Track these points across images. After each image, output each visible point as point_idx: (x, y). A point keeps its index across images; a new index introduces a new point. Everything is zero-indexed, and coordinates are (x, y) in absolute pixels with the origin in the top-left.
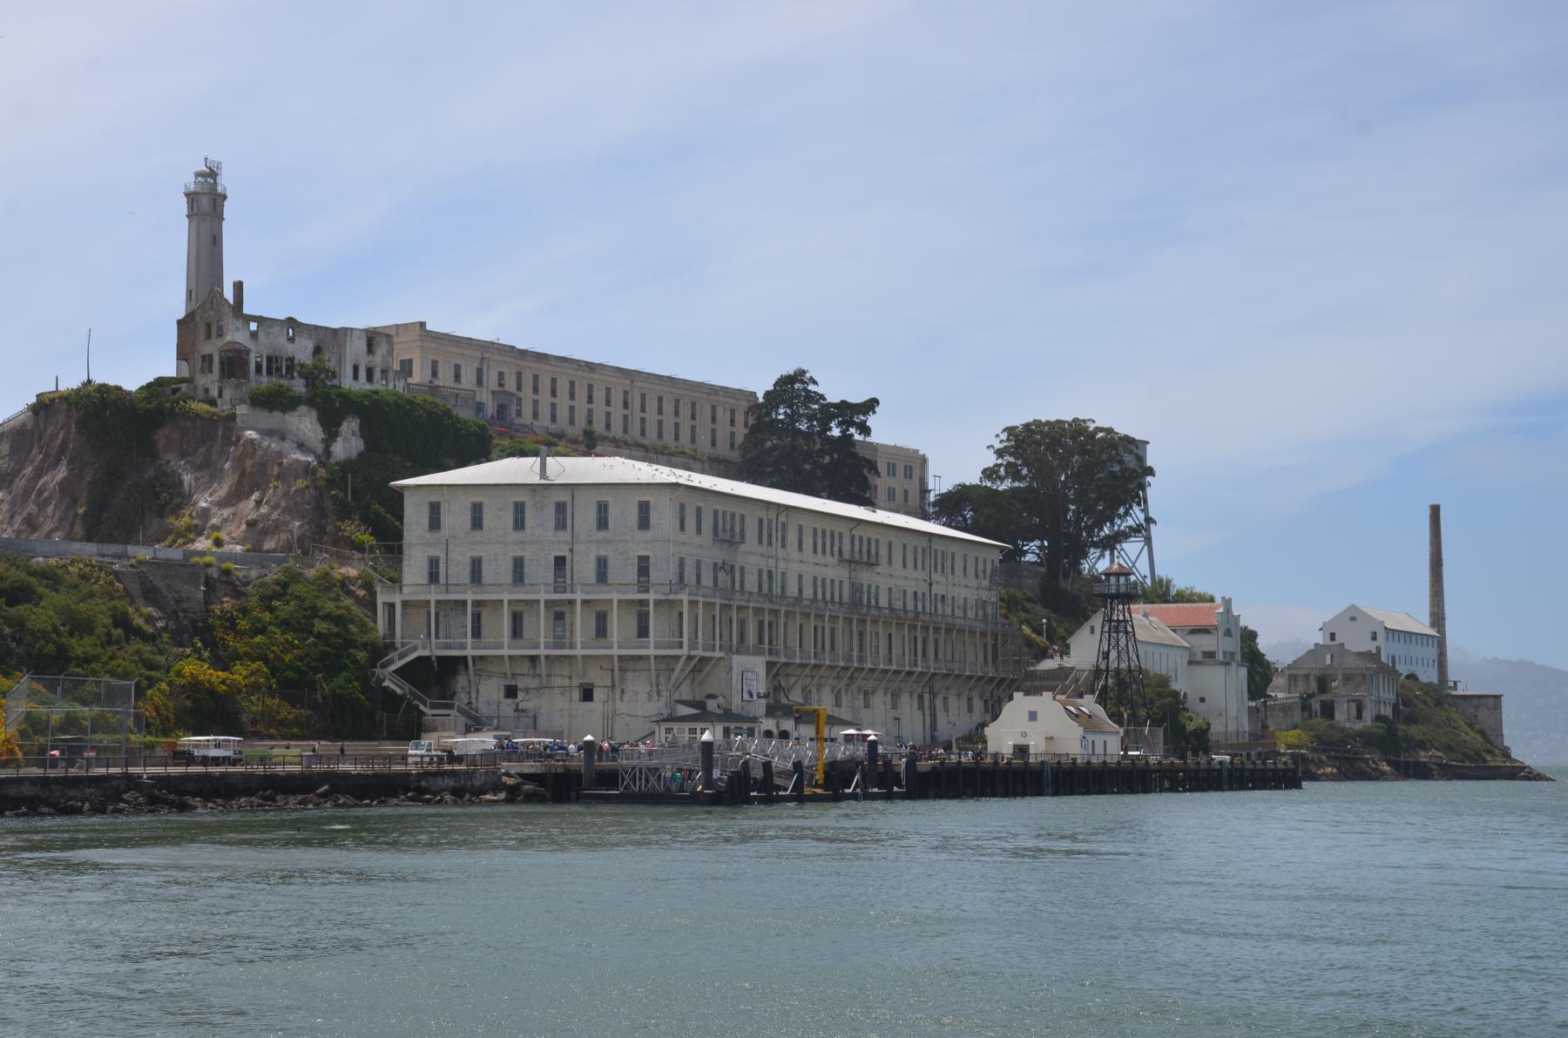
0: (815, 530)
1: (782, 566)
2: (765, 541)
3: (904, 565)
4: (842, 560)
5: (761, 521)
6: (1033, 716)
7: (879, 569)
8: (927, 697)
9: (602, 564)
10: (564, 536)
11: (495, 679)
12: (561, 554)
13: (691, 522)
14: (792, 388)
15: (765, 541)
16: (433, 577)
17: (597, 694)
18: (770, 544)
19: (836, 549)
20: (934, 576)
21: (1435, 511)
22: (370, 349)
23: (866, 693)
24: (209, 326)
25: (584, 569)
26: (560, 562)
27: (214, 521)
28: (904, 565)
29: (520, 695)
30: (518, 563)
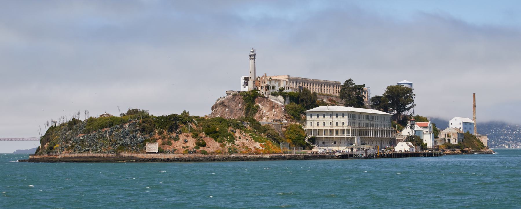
1: (361, 122)
3: (377, 120)
6: (402, 145)
8: (381, 142)
9: (337, 123)
11: (321, 141)
14: (349, 82)
16: (311, 125)
17: (337, 143)
20: (382, 121)
21: (474, 94)
22: (287, 85)
25: (334, 124)
26: (331, 123)
28: (377, 120)
29: (325, 143)
30: (324, 123)
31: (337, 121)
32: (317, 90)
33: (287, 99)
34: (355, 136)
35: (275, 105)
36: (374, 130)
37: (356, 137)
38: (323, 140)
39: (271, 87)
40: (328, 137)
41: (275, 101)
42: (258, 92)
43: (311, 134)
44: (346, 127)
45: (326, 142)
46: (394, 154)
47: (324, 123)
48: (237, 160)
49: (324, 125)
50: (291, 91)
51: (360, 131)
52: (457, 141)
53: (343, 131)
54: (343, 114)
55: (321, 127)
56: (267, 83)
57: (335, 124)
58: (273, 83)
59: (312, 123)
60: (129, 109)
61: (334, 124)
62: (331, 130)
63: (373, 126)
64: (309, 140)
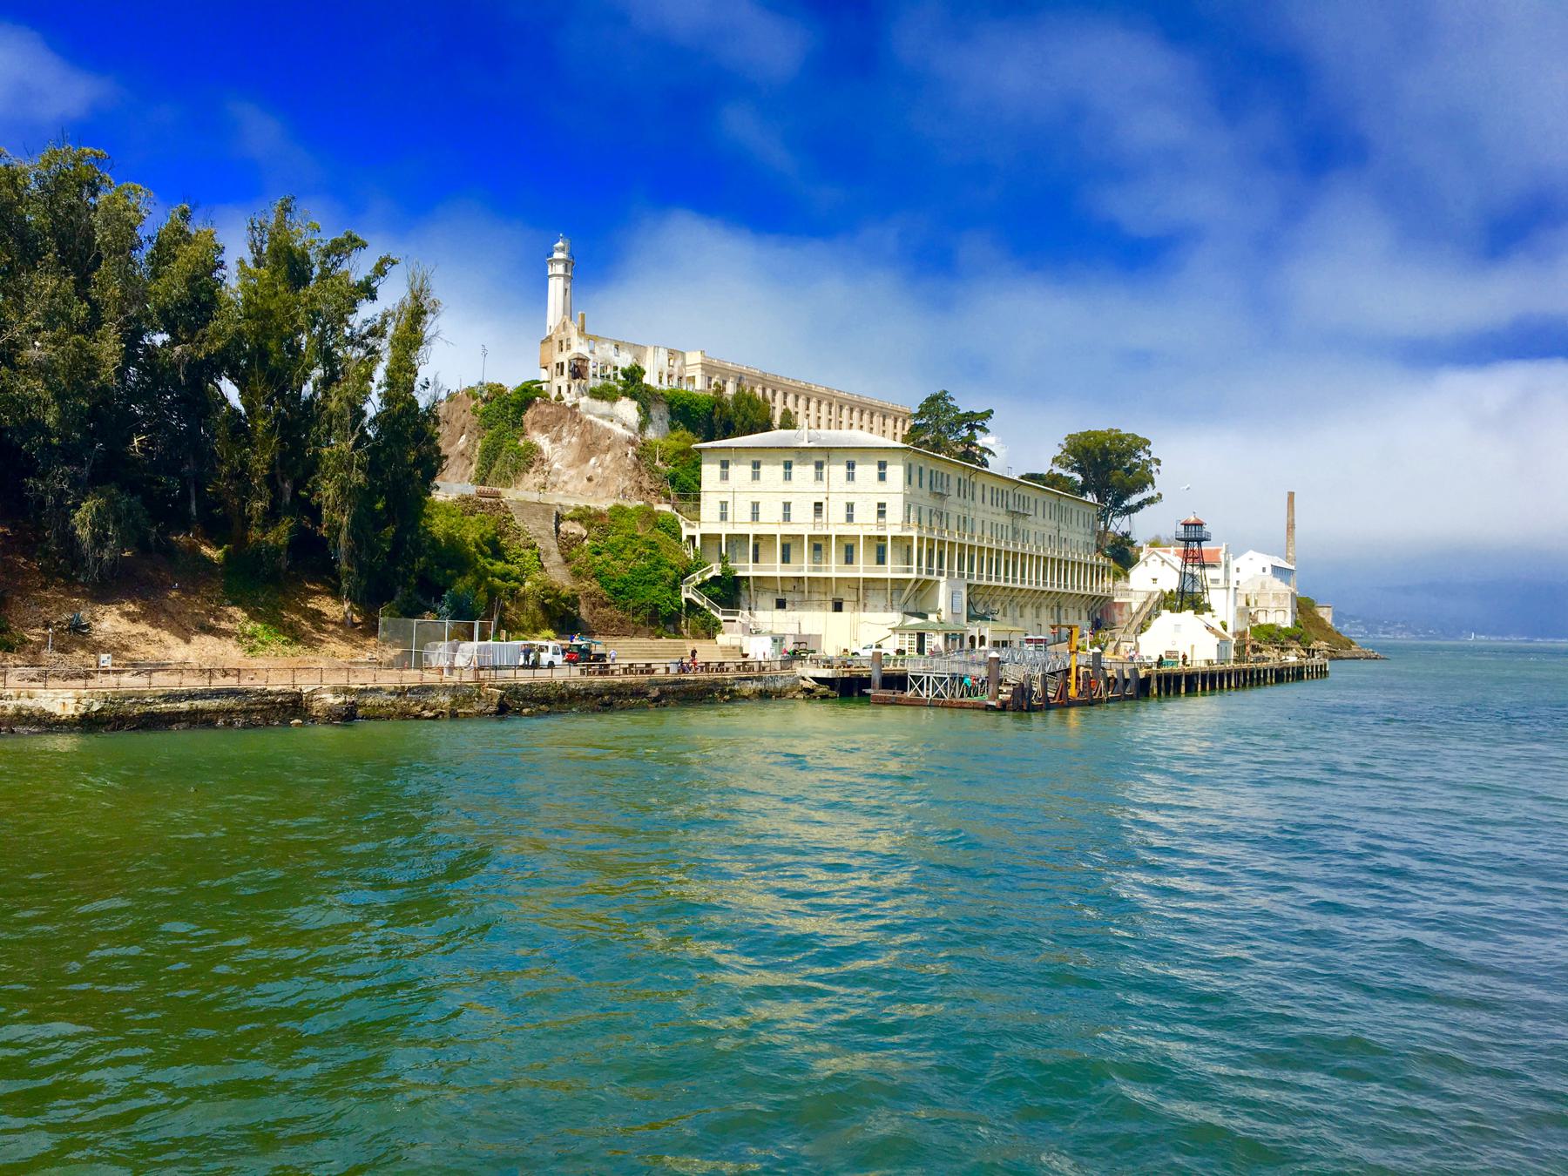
0: (992, 488)
1: (972, 513)
2: (962, 495)
4: (1008, 511)
5: (960, 480)
7: (1030, 518)
8: (1056, 609)
9: (850, 507)
10: (822, 486)
11: (769, 594)
13: (915, 478)
15: (962, 495)
16: (723, 517)
18: (965, 497)
19: (1005, 502)
21: (1291, 495)
24: (561, 342)
25: (836, 512)
26: (818, 506)
27: (565, 478)
30: (787, 506)
34: (940, 573)
35: (598, 438)
36: (1031, 556)
37: (943, 579)
41: (600, 422)
42: (541, 388)
44: (894, 526)
46: (1159, 678)
47: (787, 506)
49: (787, 517)
51: (967, 554)
53: (879, 547)
55: (771, 524)
57: (842, 513)
59: (726, 502)
61: (836, 512)
63: (1026, 539)
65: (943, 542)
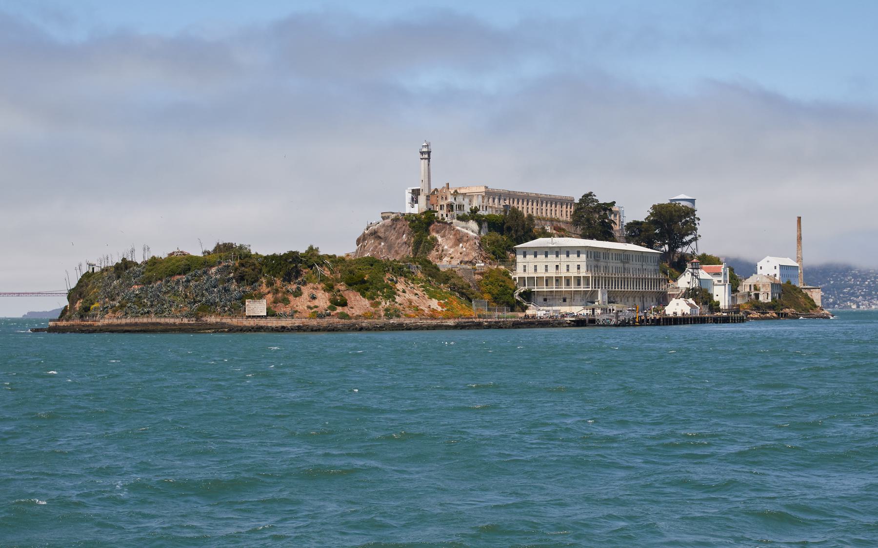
1: (608, 264)
6: (678, 304)
9: (568, 266)
12: (557, 264)
16: (525, 270)
17: (567, 300)
21: (799, 218)
23: (628, 298)
25: (563, 268)
26: (557, 266)
29: (548, 301)
30: (546, 266)
31: (568, 264)
32: (535, 210)
33: (483, 226)
34: (599, 288)
35: (463, 236)
36: (631, 278)
37: (599, 290)
38: (544, 295)
39: (456, 206)
40: (553, 290)
41: (463, 230)
42: (434, 215)
43: (525, 285)
44: (583, 273)
45: (550, 299)
46: (663, 319)
47: (546, 266)
48: (399, 330)
50: (491, 213)
51: (607, 281)
52: (770, 298)
53: (578, 280)
54: (578, 251)
55: (541, 273)
56: (451, 199)
57: (565, 268)
58: (460, 199)
59: (526, 266)
60: (218, 244)
61: (563, 268)
62: (559, 278)
63: (629, 272)
64: (520, 295)
65: (599, 277)
